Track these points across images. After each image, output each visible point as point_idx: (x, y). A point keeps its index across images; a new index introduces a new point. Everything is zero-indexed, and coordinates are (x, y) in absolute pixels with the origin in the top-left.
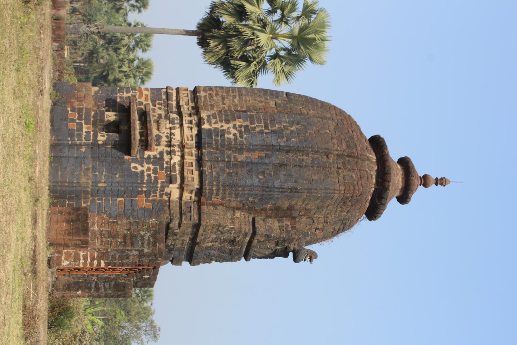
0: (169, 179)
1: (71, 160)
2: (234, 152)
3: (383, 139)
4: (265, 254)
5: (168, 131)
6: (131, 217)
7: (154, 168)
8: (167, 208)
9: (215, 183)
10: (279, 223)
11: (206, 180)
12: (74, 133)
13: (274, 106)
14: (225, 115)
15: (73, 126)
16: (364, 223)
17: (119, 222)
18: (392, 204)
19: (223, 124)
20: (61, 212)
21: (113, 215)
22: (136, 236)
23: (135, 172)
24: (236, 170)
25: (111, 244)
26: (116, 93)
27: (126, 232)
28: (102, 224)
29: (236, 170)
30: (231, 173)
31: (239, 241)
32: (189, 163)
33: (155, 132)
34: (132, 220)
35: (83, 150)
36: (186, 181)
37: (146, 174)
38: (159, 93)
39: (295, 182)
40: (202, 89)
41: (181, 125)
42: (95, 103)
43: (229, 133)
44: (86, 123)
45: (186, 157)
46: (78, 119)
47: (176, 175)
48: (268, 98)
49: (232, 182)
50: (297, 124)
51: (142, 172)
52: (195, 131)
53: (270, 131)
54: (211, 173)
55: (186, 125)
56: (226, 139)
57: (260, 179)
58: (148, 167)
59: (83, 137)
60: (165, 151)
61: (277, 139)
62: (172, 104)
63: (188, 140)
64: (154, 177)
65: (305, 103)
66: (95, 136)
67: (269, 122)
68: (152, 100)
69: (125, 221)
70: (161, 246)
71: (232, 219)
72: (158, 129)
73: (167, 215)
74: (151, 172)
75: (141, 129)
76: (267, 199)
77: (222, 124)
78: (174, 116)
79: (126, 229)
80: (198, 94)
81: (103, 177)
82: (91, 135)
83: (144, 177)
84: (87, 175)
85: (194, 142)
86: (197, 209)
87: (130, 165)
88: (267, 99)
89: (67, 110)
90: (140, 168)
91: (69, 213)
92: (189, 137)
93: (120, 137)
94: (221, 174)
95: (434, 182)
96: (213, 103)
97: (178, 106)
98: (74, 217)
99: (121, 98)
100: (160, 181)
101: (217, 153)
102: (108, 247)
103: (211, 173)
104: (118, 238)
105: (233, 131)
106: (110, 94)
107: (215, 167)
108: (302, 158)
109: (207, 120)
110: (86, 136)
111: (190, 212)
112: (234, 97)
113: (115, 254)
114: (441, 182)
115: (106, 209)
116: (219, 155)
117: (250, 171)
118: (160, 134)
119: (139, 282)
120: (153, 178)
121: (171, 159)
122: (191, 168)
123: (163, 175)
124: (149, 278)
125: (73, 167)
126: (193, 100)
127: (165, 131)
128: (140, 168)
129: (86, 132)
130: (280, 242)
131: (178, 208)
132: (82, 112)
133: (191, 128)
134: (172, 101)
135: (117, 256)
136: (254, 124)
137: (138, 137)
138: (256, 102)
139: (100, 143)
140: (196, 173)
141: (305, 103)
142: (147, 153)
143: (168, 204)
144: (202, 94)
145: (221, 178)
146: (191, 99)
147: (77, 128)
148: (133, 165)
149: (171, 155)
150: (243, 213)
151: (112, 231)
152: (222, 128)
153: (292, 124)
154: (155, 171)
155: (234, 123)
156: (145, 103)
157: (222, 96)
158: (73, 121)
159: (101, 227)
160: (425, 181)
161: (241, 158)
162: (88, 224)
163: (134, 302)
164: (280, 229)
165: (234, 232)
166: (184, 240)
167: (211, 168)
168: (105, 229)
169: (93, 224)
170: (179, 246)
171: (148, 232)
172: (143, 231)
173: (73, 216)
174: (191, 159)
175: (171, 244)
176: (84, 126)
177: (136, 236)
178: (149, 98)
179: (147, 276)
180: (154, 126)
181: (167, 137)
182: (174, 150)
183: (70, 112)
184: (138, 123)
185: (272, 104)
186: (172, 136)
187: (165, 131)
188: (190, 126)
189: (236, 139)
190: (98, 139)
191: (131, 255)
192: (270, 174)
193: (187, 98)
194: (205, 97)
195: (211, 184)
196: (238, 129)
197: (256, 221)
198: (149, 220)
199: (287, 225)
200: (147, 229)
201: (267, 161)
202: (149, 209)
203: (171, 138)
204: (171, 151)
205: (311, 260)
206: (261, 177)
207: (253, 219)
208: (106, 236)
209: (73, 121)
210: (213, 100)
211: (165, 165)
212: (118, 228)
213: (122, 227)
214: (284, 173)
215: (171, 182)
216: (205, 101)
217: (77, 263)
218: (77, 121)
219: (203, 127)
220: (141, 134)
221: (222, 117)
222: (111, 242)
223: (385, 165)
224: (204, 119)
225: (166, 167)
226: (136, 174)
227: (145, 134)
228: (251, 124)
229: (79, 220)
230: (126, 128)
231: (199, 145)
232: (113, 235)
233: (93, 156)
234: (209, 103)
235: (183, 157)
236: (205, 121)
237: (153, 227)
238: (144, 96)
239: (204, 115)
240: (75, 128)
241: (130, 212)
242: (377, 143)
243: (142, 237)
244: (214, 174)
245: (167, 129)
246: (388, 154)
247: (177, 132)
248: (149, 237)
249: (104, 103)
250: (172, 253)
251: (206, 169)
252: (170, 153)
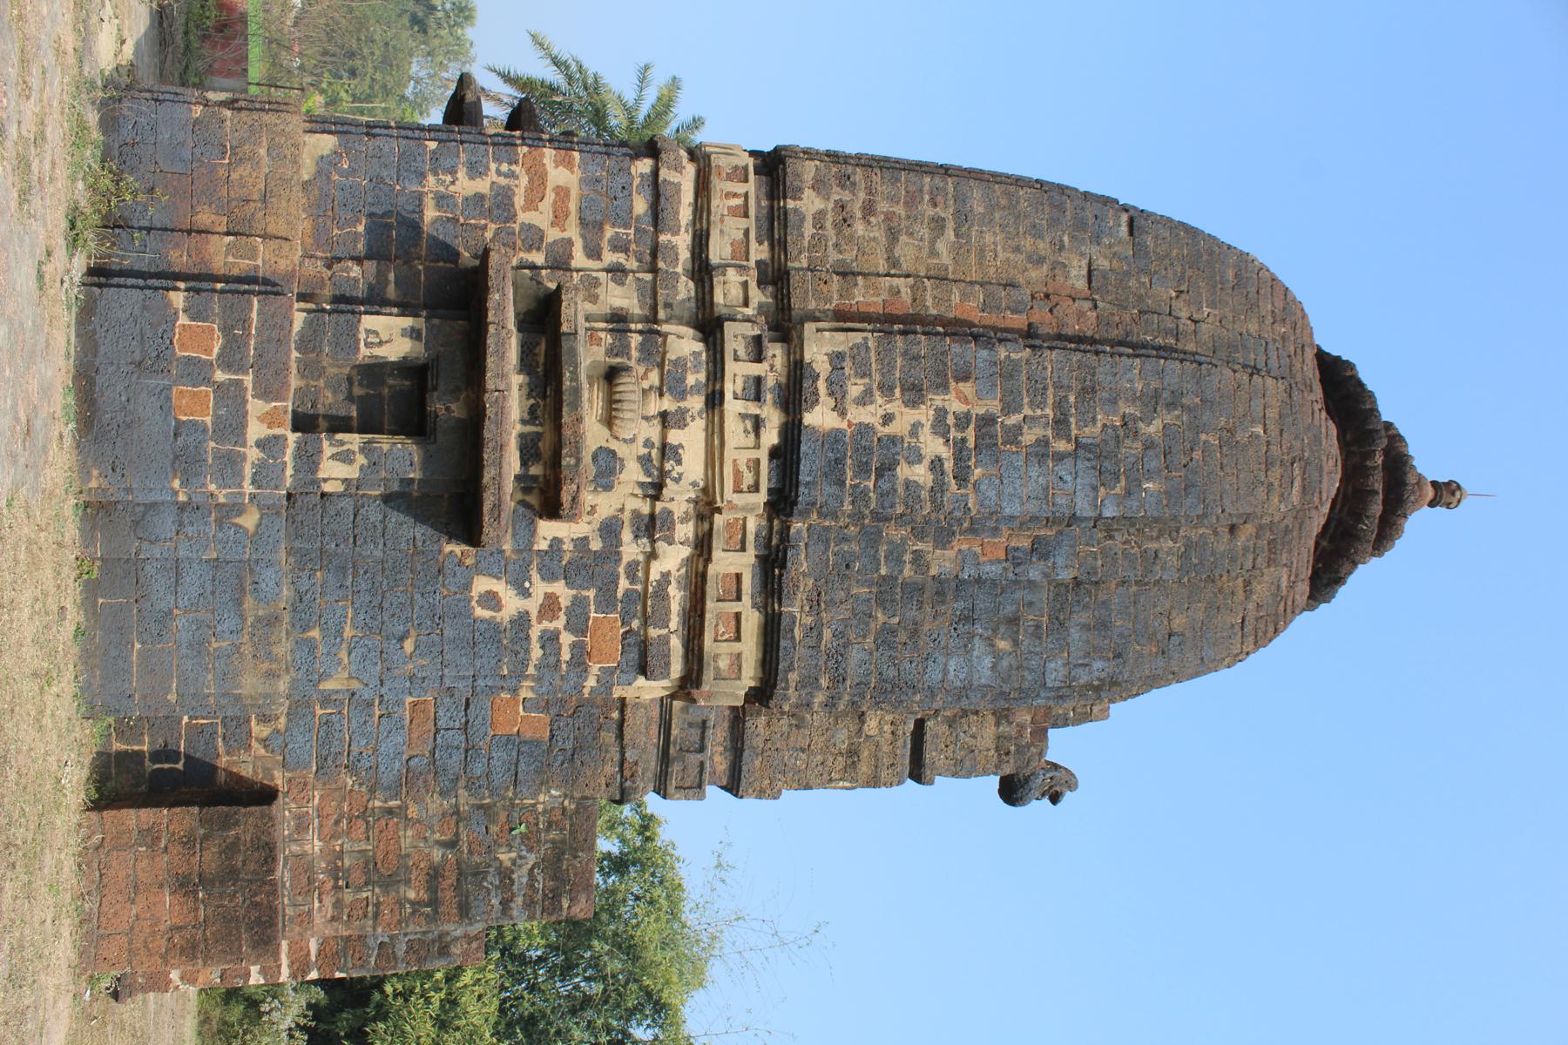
0: (634, 655)
1: (193, 580)
2: (920, 535)
3: (1371, 395)
5: (653, 431)
6: (462, 783)
7: (575, 597)
8: (609, 737)
9: (824, 682)
10: (998, 724)
11: (790, 668)
12: (199, 445)
13: (1081, 284)
14: (905, 354)
15: (196, 406)
17: (413, 811)
19: (895, 407)
20: (150, 836)
21: (386, 778)
22: (479, 874)
23: (488, 622)
24: (913, 613)
25: (376, 916)
26: (423, 176)
27: (437, 855)
28: (337, 822)
29: (913, 613)
30: (893, 632)
32: (726, 576)
33: (593, 435)
34: (464, 799)
35: (249, 520)
36: (708, 675)
37: (535, 633)
38: (621, 180)
39: (1118, 656)
40: (809, 170)
41: (714, 401)
42: (317, 231)
43: (916, 457)
44: (264, 393)
45: (717, 554)
46: (227, 365)
47: (665, 641)
48: (1066, 238)
49: (892, 672)
50: (1171, 406)
51: (522, 620)
52: (771, 437)
53: (1071, 447)
54: (815, 630)
55: (733, 407)
56: (901, 490)
57: (998, 656)
58: (548, 596)
59: (248, 471)
60: (626, 516)
61: (1095, 488)
62: (674, 248)
63: (738, 490)
64: (573, 646)
65: (1189, 272)
66: (308, 460)
67: (1072, 399)
68: (583, 222)
69: (436, 804)
70: (576, 910)
71: (853, 753)
72: (609, 421)
73: (611, 769)
74: (560, 623)
75: (532, 416)
77: (890, 408)
78: (684, 344)
79: (438, 842)
80: (791, 204)
81: (343, 655)
82: (289, 451)
83: (527, 651)
84: (270, 657)
85: (762, 497)
86: (726, 724)
87: (467, 586)
88: (1062, 247)
89: (169, 304)
90: (512, 603)
91: (189, 842)
92: (743, 468)
93: (426, 462)
94: (852, 637)
95: (1430, 493)
96: (849, 256)
97: (702, 271)
98: (209, 859)
99: (442, 200)
100: (595, 669)
101: (846, 539)
102: (363, 927)
103: (815, 630)
104: (408, 882)
105: (933, 446)
106: (388, 174)
107: (832, 603)
108: (1153, 546)
109: (830, 382)
110: (260, 468)
111: (702, 749)
112: (938, 225)
113: (392, 937)
114: (1445, 494)
115: (355, 749)
116: (855, 547)
117: (967, 619)
118: (614, 445)
120: (566, 655)
121: (652, 555)
122: (734, 607)
123: (608, 628)
125: (202, 615)
126: (766, 225)
127: (639, 431)
128: (512, 603)
129: (260, 444)
131: (654, 729)
132: (245, 322)
133: (758, 424)
134: (676, 233)
135: (401, 949)
136: (1018, 410)
137: (513, 463)
138: (1020, 258)
139: (327, 488)
140: (752, 621)
141: (1189, 272)
142: (548, 530)
143: (615, 715)
144: (808, 203)
145: (855, 655)
146: (758, 228)
147: (217, 417)
148: (482, 585)
149: (653, 542)
150: (889, 718)
151: (380, 856)
152: (887, 430)
153: (1152, 402)
154: (577, 622)
155: (938, 400)
156: (553, 235)
157: (889, 217)
158: (197, 371)
159: (334, 836)
161: (942, 562)
162: (274, 889)
163: (440, 26)
164: (997, 749)
167: (815, 603)
168: (353, 845)
169: (302, 825)
171: (530, 850)
172: (510, 848)
173: (207, 856)
174: (734, 562)
176: (256, 407)
177: (479, 874)
178: (573, 206)
180: (592, 403)
181: (645, 461)
182: (670, 513)
183: (183, 320)
184: (517, 380)
185: (1077, 278)
186: (668, 467)
187: (639, 431)
188: (753, 409)
189: (939, 488)
190: (321, 475)
191: (456, 939)
192: (1038, 627)
193: (743, 223)
194: (819, 217)
195: (809, 682)
196: (953, 433)
197: (928, 737)
198: (535, 795)
199: (1021, 727)
200: (524, 836)
201: (1034, 574)
202: (537, 743)
203: (663, 474)
204: (652, 516)
205: (1055, 799)
206: (1003, 645)
207: (920, 725)
208: (357, 877)
209: (197, 371)
210: (851, 239)
211: (623, 584)
212: (408, 837)
213: (419, 841)
214: (1083, 617)
215: (643, 670)
216: (818, 241)
218: (220, 376)
219: (809, 418)
220: (529, 451)
221: (891, 366)
222: (377, 905)
223: (1365, 509)
224: (816, 377)
225: (627, 593)
226: (494, 627)
227: (545, 446)
228: (1008, 409)
229: (232, 874)
230: (458, 410)
231: (782, 502)
232: (381, 874)
233: (297, 544)
234: (834, 256)
235: (703, 546)
236: (822, 386)
237: (550, 825)
238: (550, 196)
239: (819, 348)
240: (208, 420)
241: (458, 757)
243: (506, 875)
244: (827, 634)
245: (646, 418)
247: (691, 439)
248: (532, 869)
249: (361, 228)
251: (796, 610)
252: (651, 527)
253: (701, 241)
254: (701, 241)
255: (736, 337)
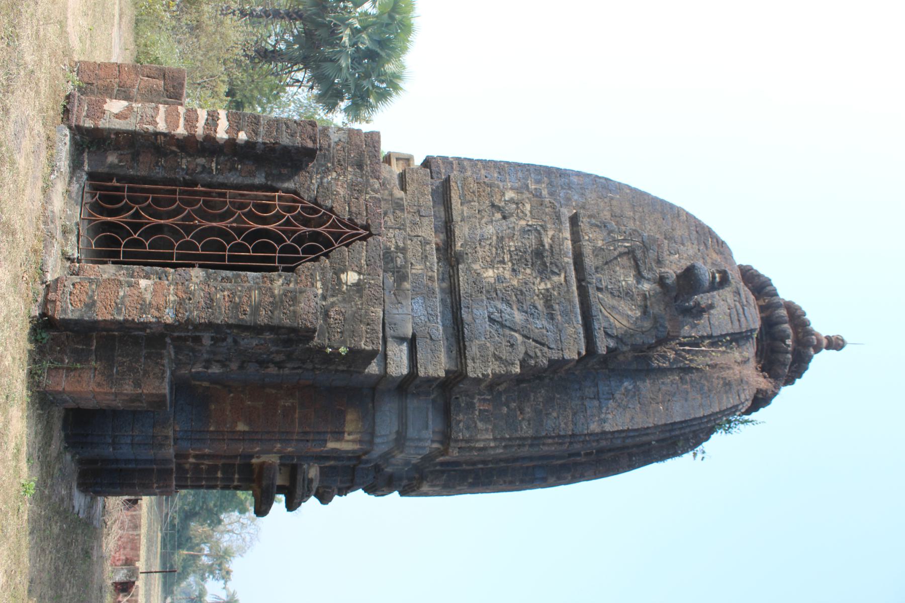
4: (628, 316)
31: (551, 246)
76: (562, 188)
119: (333, 304)
124: (358, 286)
130: (639, 254)
165: (528, 207)
166: (428, 243)
170: (418, 268)
175: (397, 247)
179: (351, 277)
217: (150, 112)
250: (406, 297)
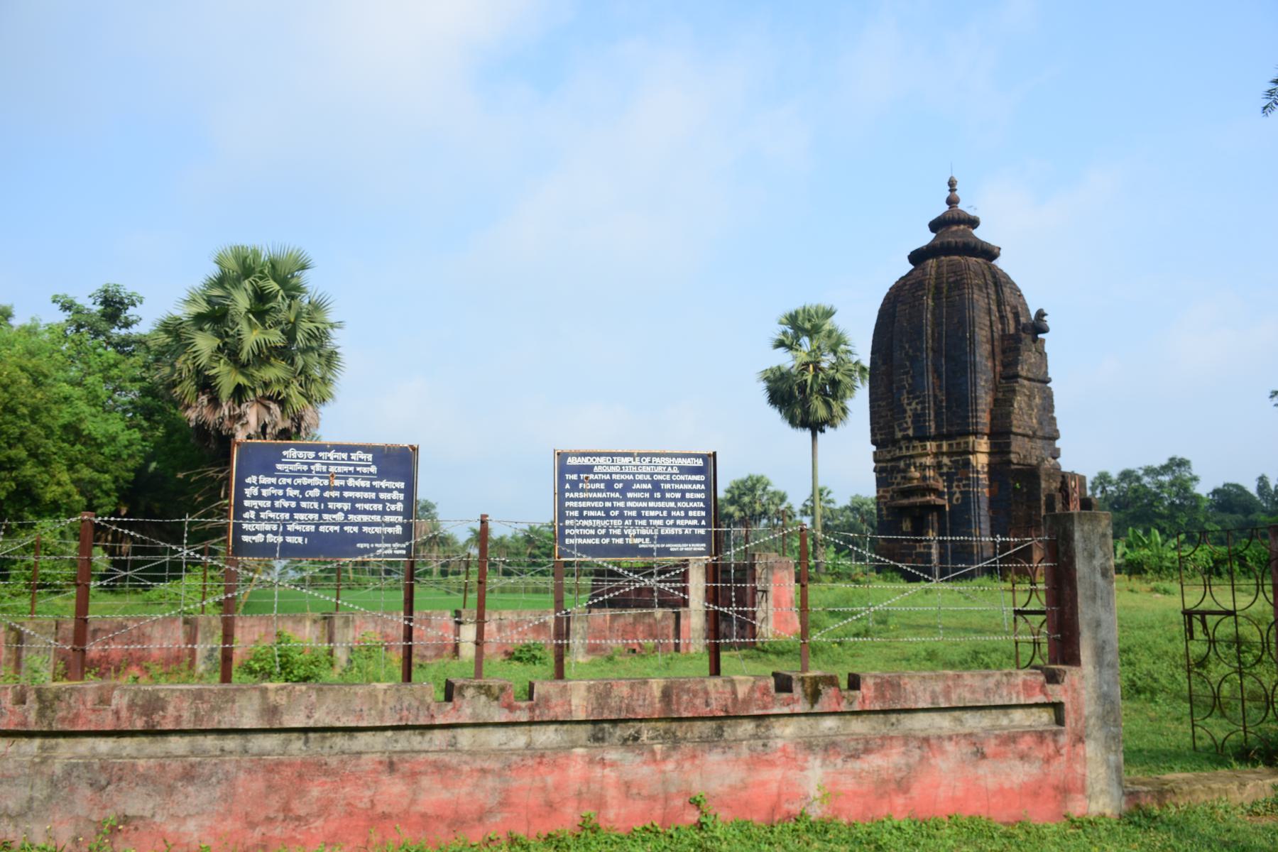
16: (1001, 263)
18: (980, 233)
41: (912, 457)
51: (961, 492)
52: (916, 443)
55: (911, 452)
78: (902, 464)
90: (958, 495)
105: (914, 405)
114: (952, 184)
128: (958, 495)
154: (960, 480)
160: (952, 202)
226: (963, 498)
242: (917, 257)
246: (927, 246)
253: (888, 461)
254: (888, 461)
255: (898, 453)
